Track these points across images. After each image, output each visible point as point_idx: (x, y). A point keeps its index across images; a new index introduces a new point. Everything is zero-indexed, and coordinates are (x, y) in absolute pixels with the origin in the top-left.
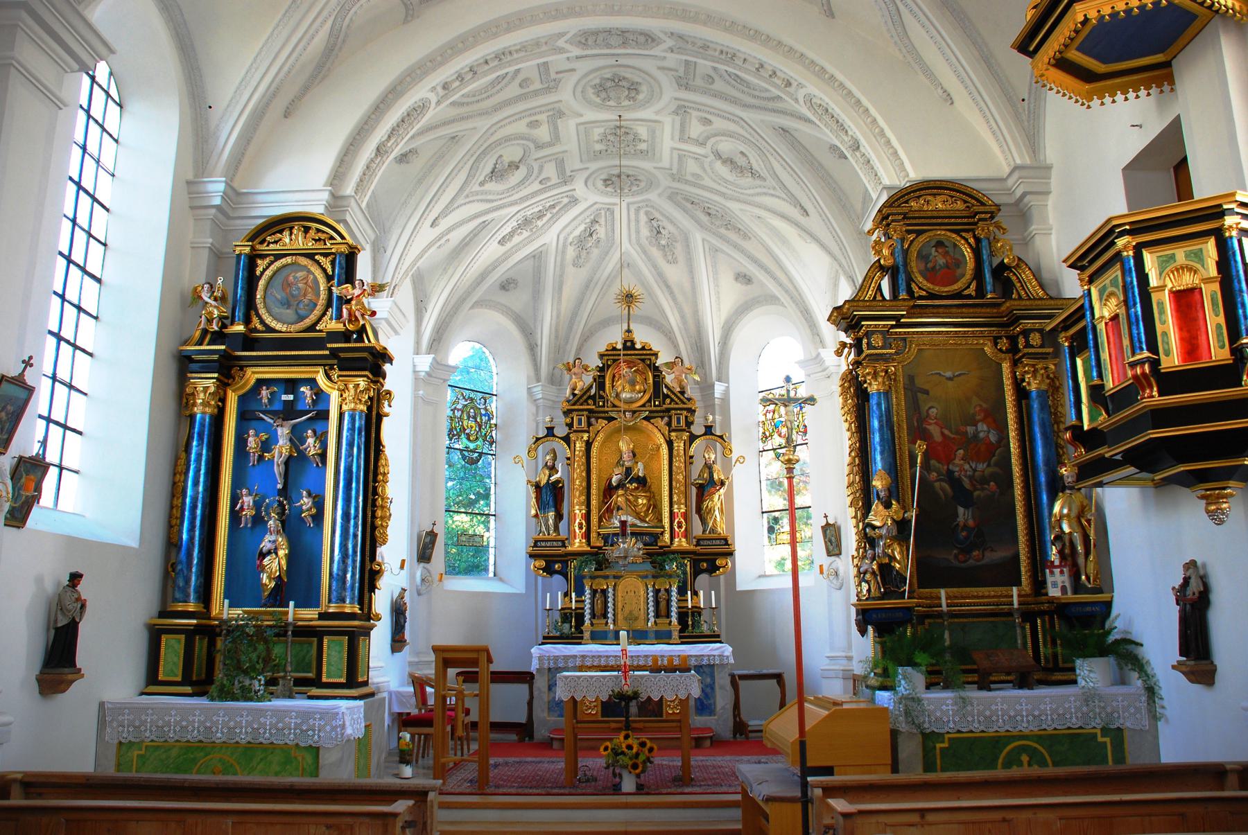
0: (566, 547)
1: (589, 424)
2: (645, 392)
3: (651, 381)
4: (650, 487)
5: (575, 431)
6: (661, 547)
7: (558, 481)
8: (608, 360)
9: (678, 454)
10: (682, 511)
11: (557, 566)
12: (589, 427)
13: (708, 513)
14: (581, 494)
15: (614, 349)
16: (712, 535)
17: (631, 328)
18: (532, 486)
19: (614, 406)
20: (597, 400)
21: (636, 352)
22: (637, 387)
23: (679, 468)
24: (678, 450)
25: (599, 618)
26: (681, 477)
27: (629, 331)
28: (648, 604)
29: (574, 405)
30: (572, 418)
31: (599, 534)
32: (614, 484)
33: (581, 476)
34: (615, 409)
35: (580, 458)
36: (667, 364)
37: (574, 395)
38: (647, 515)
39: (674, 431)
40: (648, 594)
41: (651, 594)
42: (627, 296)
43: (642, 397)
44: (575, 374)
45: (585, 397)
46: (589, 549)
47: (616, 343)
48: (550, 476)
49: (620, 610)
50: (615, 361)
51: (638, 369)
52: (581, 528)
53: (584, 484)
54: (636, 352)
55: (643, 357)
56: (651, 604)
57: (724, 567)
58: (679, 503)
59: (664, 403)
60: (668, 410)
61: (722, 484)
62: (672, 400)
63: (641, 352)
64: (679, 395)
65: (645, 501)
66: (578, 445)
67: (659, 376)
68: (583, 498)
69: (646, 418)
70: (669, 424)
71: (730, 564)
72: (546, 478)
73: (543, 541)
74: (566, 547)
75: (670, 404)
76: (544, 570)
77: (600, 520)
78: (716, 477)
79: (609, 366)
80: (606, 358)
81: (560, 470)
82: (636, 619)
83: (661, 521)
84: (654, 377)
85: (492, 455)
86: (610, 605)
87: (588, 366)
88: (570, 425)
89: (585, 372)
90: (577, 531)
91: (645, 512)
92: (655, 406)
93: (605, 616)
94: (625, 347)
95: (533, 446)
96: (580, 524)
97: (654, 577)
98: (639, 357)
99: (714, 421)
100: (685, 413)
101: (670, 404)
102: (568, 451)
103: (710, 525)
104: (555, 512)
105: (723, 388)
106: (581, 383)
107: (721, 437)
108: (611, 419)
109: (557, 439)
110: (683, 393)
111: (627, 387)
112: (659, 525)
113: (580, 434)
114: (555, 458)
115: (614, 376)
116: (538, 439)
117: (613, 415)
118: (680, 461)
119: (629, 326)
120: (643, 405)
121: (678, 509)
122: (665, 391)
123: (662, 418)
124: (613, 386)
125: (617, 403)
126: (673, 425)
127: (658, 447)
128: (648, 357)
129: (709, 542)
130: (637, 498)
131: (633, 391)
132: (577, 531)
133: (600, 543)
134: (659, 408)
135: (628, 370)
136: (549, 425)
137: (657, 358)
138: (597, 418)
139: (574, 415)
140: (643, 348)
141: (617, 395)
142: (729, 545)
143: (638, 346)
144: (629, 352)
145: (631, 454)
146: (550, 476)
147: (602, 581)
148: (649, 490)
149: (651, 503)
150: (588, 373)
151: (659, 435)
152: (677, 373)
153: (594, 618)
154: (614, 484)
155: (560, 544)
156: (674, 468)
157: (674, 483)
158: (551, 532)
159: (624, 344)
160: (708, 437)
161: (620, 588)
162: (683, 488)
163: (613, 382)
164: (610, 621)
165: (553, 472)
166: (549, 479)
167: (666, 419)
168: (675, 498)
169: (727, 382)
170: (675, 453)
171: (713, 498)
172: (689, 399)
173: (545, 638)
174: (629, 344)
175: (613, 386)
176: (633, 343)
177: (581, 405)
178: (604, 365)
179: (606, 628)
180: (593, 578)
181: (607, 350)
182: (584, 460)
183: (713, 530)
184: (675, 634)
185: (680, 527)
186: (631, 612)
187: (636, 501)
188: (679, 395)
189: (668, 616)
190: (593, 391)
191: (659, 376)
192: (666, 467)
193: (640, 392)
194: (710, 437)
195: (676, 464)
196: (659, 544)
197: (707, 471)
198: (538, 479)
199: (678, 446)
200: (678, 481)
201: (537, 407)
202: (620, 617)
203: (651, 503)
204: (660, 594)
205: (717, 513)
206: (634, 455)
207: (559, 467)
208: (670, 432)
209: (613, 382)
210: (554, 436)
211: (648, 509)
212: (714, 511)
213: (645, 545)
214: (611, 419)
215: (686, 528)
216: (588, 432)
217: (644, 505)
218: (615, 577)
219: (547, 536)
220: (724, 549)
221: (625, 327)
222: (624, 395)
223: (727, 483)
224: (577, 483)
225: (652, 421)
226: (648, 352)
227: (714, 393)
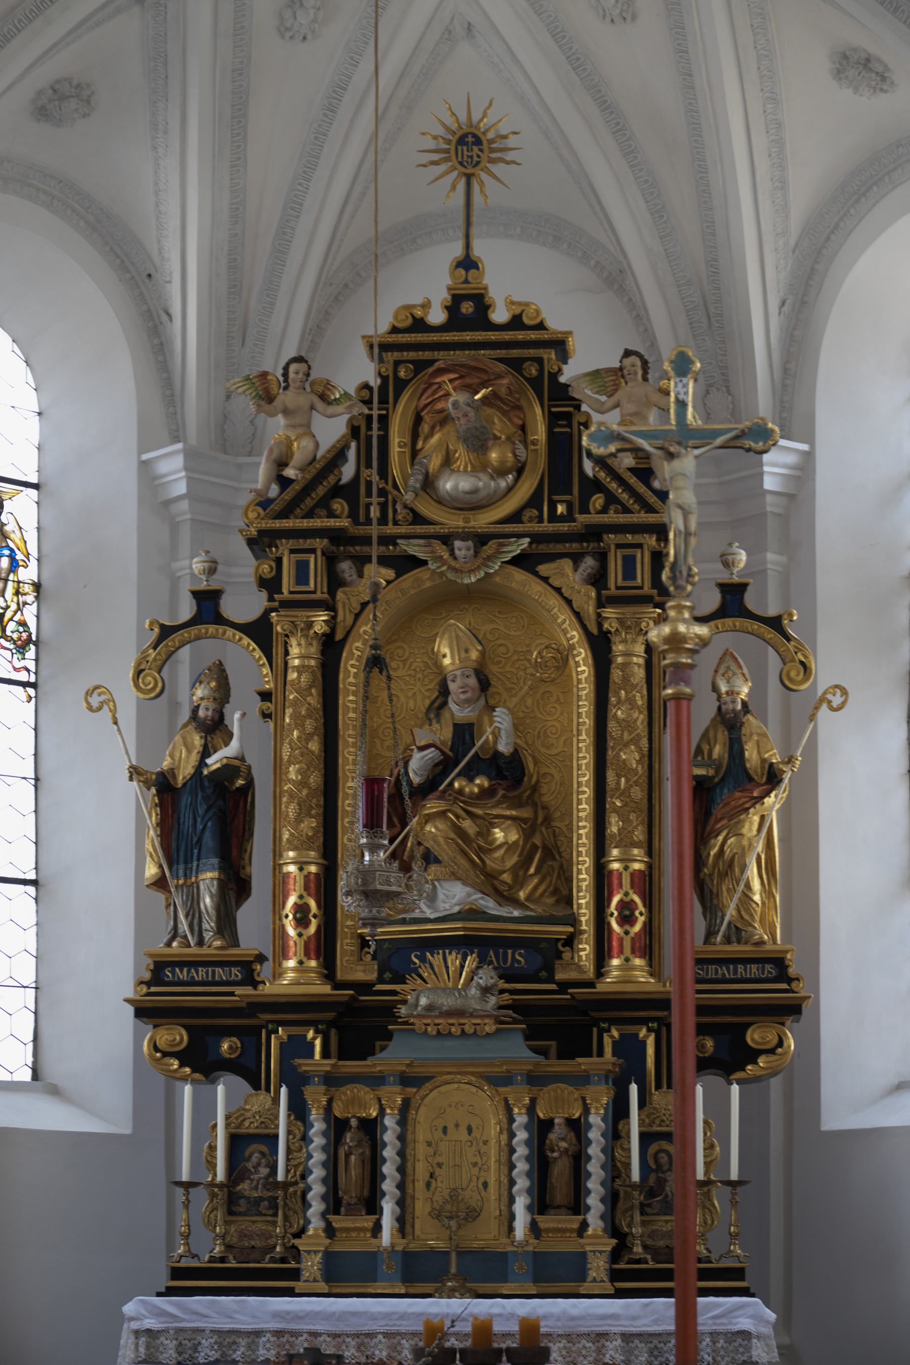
0: (255, 984)
1: (335, 582)
2: (520, 471)
3: (540, 432)
4: (535, 788)
6: (564, 986)
7: (230, 770)
9: (626, 679)
10: (637, 866)
11: (225, 1046)
12: (332, 592)
13: (723, 875)
14: (304, 811)
15: (420, 325)
16: (735, 948)
18: (147, 784)
19: (418, 518)
22: (494, 455)
23: (627, 725)
25: (352, 1211)
26: (631, 757)
27: (468, 263)
28: (512, 1167)
29: (284, 514)
30: (279, 561)
31: (364, 943)
32: (416, 780)
35: (303, 692)
36: (595, 375)
37: (284, 483)
38: (519, 882)
39: (614, 601)
40: (512, 1135)
41: (522, 1135)
42: (462, 141)
43: (510, 489)
44: (286, 412)
45: (321, 491)
46: (327, 989)
47: (426, 305)
48: (206, 753)
49: (420, 1185)
50: (420, 366)
51: (494, 394)
52: (302, 921)
55: (515, 353)
56: (522, 1167)
58: (626, 843)
59: (585, 510)
60: (595, 533)
61: (773, 778)
62: (611, 499)
63: (508, 336)
64: (633, 480)
65: (514, 837)
66: (295, 650)
67: (568, 417)
68: (310, 825)
69: (521, 561)
71: (791, 1043)
72: (194, 758)
73: (182, 964)
74: (255, 984)
75: (604, 510)
76: (184, 1057)
78: (751, 754)
79: (401, 385)
80: (391, 357)
81: (236, 730)
82: (472, 1215)
84: (553, 419)
85: (25, 685)
86: (388, 1169)
87: (328, 385)
88: (270, 585)
89: (319, 405)
90: (291, 932)
91: (514, 870)
92: (553, 517)
93: (372, 1206)
94: (455, 320)
95: (152, 654)
97: (535, 1080)
98: (502, 353)
99: (757, 569)
101: (604, 510)
102: (266, 670)
103: (731, 912)
104: (222, 869)
105: (791, 459)
106: (307, 443)
107: (775, 623)
108: (410, 563)
109: (230, 632)
111: (462, 454)
112: (560, 912)
114: (223, 694)
116: (166, 632)
117: (414, 548)
118: (631, 701)
119: (468, 246)
120: (515, 517)
121: (625, 860)
124: (414, 453)
125: (427, 509)
126: (612, 584)
127: (563, 659)
128: (532, 352)
129: (723, 971)
130: (487, 824)
131: (481, 467)
132: (291, 932)
134: (564, 527)
136: (203, 586)
137: (564, 356)
139: (284, 548)
140: (516, 323)
141: (428, 484)
143: (500, 315)
144: (468, 336)
145: (473, 681)
146: (206, 753)
147: (364, 1093)
148: (532, 799)
149: (537, 840)
150: (331, 410)
151: (564, 617)
152: (630, 408)
153: (337, 1212)
154: (416, 780)
155: (236, 973)
156: (612, 726)
157: (611, 776)
158: (208, 936)
159: (453, 308)
160: (729, 622)
161: (422, 1117)
162: (638, 793)
163: (415, 436)
164: (387, 1221)
165: (218, 739)
166: (202, 764)
167: (589, 563)
168: (614, 826)
169: (809, 437)
170: (616, 675)
171: (740, 823)
173: (177, 1273)
175: (414, 453)
177: (309, 515)
178: (384, 379)
179: (370, 1245)
180: (331, 1081)
181: (394, 330)
182: (314, 699)
183: (736, 933)
184: (598, 1267)
185: (627, 919)
186: (454, 1194)
187: (485, 833)
188: (633, 480)
189: (577, 1206)
190: (348, 471)
191: (568, 417)
192: (587, 721)
193: (501, 472)
194: (739, 622)
196: (559, 976)
197: (722, 735)
198: (166, 764)
199: (628, 654)
200: (624, 769)
201: (174, 527)
202: (421, 1208)
203: (537, 840)
204: (552, 1136)
205: (752, 872)
206: (484, 684)
207: (235, 721)
208: (601, 603)
209: (415, 436)
210: (220, 620)
211: (526, 862)
212: (744, 867)
213: (506, 976)
214: (410, 563)
215: (649, 926)
216: (330, 606)
217: (510, 847)
218: (406, 1080)
219: (194, 950)
220: (773, 993)
222: (448, 485)
223: (787, 777)
224: (292, 776)
225: (543, 569)
226: (533, 335)
227: (761, 475)
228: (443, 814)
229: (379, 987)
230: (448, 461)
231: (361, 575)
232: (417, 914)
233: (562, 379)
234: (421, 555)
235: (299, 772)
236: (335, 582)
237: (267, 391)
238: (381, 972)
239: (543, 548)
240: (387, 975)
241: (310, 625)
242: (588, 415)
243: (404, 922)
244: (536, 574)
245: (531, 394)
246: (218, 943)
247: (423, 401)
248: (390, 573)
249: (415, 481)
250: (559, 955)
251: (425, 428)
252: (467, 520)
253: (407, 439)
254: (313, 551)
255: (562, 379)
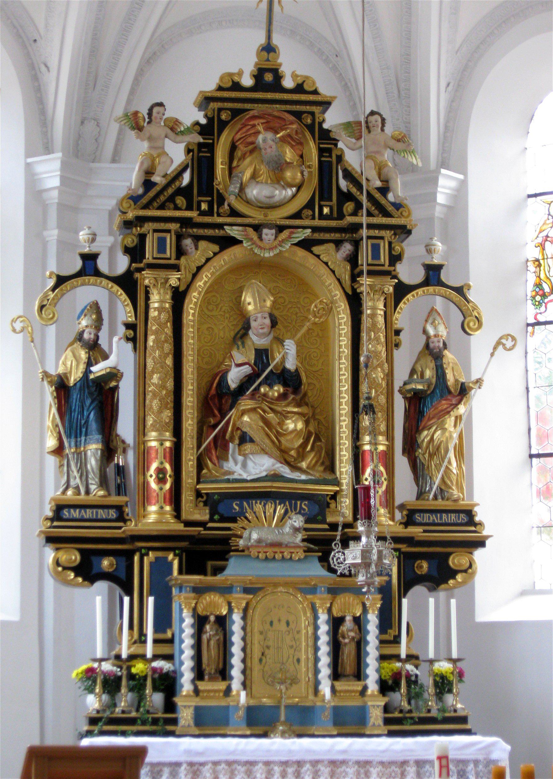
1: (180, 252)
5: (151, 266)
8: (220, 110)
10: (381, 448)
13: (431, 456)
15: (236, 86)
16: (440, 504)
17: (276, 40)
19: (234, 213)
20: (196, 199)
21: (286, 96)
24: (373, 316)
31: (198, 494)
33: (163, 365)
34: (239, 220)
36: (348, 126)
43: (294, 196)
47: (240, 73)
50: (236, 113)
53: (170, 384)
54: (286, 96)
57: (465, 571)
68: (167, 415)
70: (353, 260)
77: (200, 466)
79: (223, 125)
83: (331, 468)
84: (321, 151)
87: (177, 122)
90: (154, 485)
91: (297, 450)
92: (322, 217)
96: (161, 471)
98: (289, 107)
100: (387, 234)
110: (384, 190)
113: (162, 274)
115: (233, 148)
117: (234, 232)
118: (377, 339)
120: (297, 215)
121: (374, 443)
122: (343, 184)
123: (338, 243)
127: (329, 309)
128: (308, 108)
133: (202, 515)
135: (270, 135)
138: (197, 239)
140: (299, 89)
142: (475, 524)
143: (288, 83)
144: (269, 96)
149: (311, 429)
151: (330, 280)
159: (259, 75)
172: (398, 206)
174: (269, 77)
176: (278, 76)
181: (220, 88)
183: (442, 492)
187: (281, 424)
191: (329, 151)
192: (346, 351)
195: (366, 348)
196: (329, 519)
199: (374, 308)
205: (451, 454)
212: (447, 451)
221: (262, 40)
225: (316, 249)
228: (254, 410)
229: (210, 525)
230: (254, 176)
231: (197, 248)
232: (236, 476)
233: (325, 126)
234: (239, 238)
235: (160, 379)
236: (180, 252)
237: (137, 124)
238: (212, 515)
239: (317, 236)
240: (216, 517)
241: (167, 280)
242: (342, 150)
243: (228, 481)
244: (311, 252)
245: (308, 134)
246: (101, 493)
247: (238, 136)
248: (216, 248)
249: (234, 188)
250: (328, 505)
251: (238, 153)
252: (266, 215)
253: (227, 160)
254: (169, 231)
255: (325, 126)
